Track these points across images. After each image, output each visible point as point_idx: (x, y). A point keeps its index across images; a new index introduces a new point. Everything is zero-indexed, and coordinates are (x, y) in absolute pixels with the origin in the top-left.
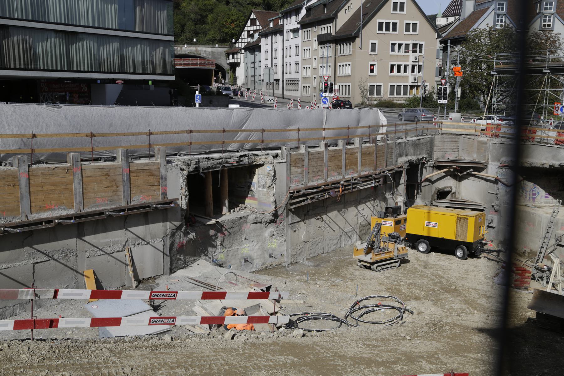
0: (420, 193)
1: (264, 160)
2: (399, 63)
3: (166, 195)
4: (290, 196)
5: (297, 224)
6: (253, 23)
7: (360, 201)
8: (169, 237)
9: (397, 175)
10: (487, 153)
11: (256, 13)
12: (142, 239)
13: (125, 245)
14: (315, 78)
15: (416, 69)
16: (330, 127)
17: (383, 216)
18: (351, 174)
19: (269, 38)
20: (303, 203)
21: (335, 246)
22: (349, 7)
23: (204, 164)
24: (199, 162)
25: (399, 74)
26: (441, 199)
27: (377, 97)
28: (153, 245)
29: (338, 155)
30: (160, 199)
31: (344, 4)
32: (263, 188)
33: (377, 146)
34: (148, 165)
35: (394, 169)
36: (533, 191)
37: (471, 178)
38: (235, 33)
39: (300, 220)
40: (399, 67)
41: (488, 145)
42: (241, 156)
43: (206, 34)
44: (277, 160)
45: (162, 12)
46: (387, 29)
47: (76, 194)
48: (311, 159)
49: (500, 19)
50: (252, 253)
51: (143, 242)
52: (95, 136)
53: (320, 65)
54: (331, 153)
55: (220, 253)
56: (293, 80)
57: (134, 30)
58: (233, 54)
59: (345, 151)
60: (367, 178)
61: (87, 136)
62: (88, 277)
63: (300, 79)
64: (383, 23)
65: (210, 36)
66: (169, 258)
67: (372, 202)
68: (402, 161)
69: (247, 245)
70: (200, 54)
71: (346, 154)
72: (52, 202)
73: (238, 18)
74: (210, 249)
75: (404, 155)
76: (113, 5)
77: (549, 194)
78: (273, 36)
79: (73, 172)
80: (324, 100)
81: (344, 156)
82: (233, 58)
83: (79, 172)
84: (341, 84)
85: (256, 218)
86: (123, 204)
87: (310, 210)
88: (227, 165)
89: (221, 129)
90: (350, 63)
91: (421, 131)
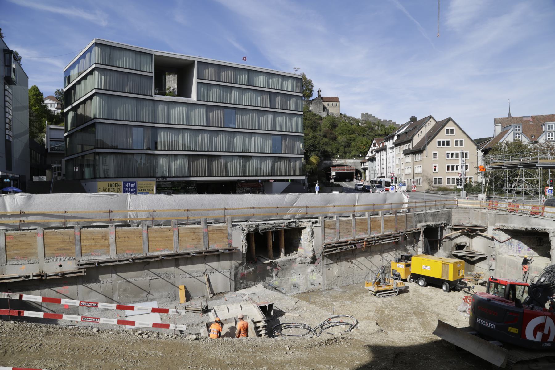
0: (442, 246)
1: (306, 225)
3: (232, 244)
4: (325, 247)
5: (331, 265)
6: (375, 146)
7: (384, 251)
8: (233, 269)
9: (416, 235)
11: (376, 140)
12: (215, 270)
13: (205, 272)
17: (398, 261)
19: (379, 153)
20: (334, 252)
21: (363, 280)
23: (262, 227)
24: (258, 226)
25: (453, 171)
26: (459, 249)
27: (439, 185)
28: (223, 273)
30: (228, 247)
33: (397, 216)
36: (518, 246)
37: (478, 236)
39: (333, 262)
40: (453, 167)
41: (487, 215)
44: (315, 225)
47: (174, 243)
48: (341, 224)
49: (518, 136)
50: (298, 282)
51: (216, 272)
52: (189, 211)
53: (405, 167)
55: (275, 280)
57: (280, 153)
58: (364, 163)
59: (369, 219)
60: (388, 236)
61: (185, 211)
62: (181, 290)
65: (353, 154)
66: (234, 282)
67: (394, 252)
68: (421, 226)
69: (295, 277)
71: (371, 221)
72: (161, 247)
73: (367, 143)
74: (268, 278)
77: (531, 248)
79: (173, 230)
80: (392, 188)
81: (369, 222)
82: (364, 165)
83: (177, 230)
84: (417, 178)
85: (301, 260)
86: (204, 249)
88: (279, 228)
89: (275, 206)
90: (421, 165)
91: (443, 206)
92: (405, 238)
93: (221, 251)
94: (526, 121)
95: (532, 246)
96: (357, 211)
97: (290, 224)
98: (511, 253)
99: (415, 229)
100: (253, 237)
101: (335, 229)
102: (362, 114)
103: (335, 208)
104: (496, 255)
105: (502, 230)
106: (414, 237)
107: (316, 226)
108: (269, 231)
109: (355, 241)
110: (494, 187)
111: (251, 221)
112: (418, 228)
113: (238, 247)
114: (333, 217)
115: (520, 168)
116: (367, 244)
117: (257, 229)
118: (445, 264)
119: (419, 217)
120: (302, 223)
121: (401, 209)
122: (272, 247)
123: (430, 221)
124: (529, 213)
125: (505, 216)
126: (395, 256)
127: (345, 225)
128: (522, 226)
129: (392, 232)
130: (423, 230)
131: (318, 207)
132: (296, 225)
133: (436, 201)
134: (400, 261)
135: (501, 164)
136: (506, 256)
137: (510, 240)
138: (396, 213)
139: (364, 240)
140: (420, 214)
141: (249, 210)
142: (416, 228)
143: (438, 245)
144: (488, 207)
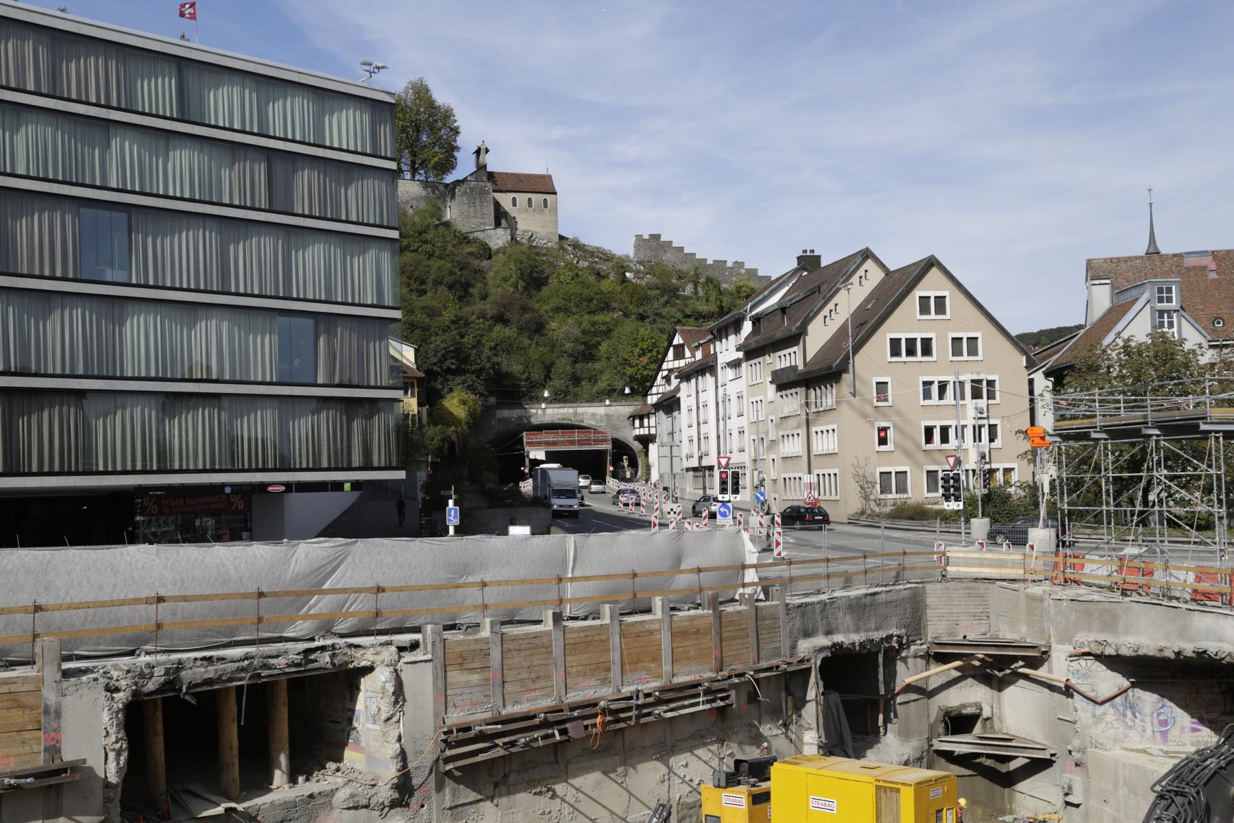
0: (895, 720)
1: (371, 658)
3: (59, 751)
4: (442, 741)
5: (471, 809)
6: (679, 354)
7: (674, 746)
9: (794, 681)
10: (1046, 624)
14: (773, 460)
16: (588, 574)
17: (723, 783)
18: (641, 682)
19: (693, 381)
22: (831, 311)
23: (195, 674)
24: (178, 670)
26: (954, 733)
27: (898, 496)
29: (596, 638)
30: (40, 762)
31: (819, 306)
32: (375, 722)
33: (719, 616)
34: (6, 683)
35: (778, 667)
36: (1159, 715)
37: (1021, 682)
38: (648, 375)
39: (480, 797)
41: (1046, 604)
42: (308, 652)
43: (596, 381)
44: (408, 657)
45: (377, 343)
46: (911, 352)
49: (1166, 320)
53: (781, 433)
54: (575, 635)
56: (739, 466)
57: (312, 381)
58: (641, 418)
59: (617, 629)
63: (747, 464)
64: (900, 339)
65: (602, 384)
67: (714, 747)
70: (582, 421)
71: (622, 635)
75: (820, 632)
76: (268, 336)
77: (1202, 721)
78: (700, 378)
80: (722, 510)
81: (615, 640)
82: (642, 426)
84: (821, 472)
85: (352, 796)
87: (510, 772)
88: (264, 673)
89: (253, 589)
90: (834, 427)
91: (894, 573)
92: (753, 697)
93: (6, 780)
94: (1194, 268)
95: (1205, 716)
96: (569, 601)
97: (312, 657)
98: (1135, 740)
99: (788, 660)
100: (159, 713)
101: (486, 668)
102: (639, 237)
103: (486, 589)
104: (1082, 750)
105: (1100, 658)
106: (787, 689)
107: (412, 659)
108: (227, 689)
109: (562, 711)
110: (1069, 504)
111: (148, 653)
112: (802, 655)
113: (84, 761)
114: (478, 625)
115: (1151, 436)
116: (610, 722)
117: (172, 682)
118: (885, 788)
119: (803, 615)
120: (360, 652)
121: (736, 587)
122: (235, 752)
123: (847, 631)
124: (1188, 597)
125: (1106, 606)
126: (715, 763)
127: (523, 653)
128: (1163, 645)
129: (702, 673)
130: (819, 663)
131: (421, 589)
132: (335, 661)
133: (790, 563)
134: (732, 780)
135: (1086, 423)
136: (1117, 752)
137: (1130, 692)
138: (715, 603)
139: (598, 709)
140: (807, 604)
141: (142, 607)
142: (792, 655)
143: (881, 717)
144: (1049, 574)
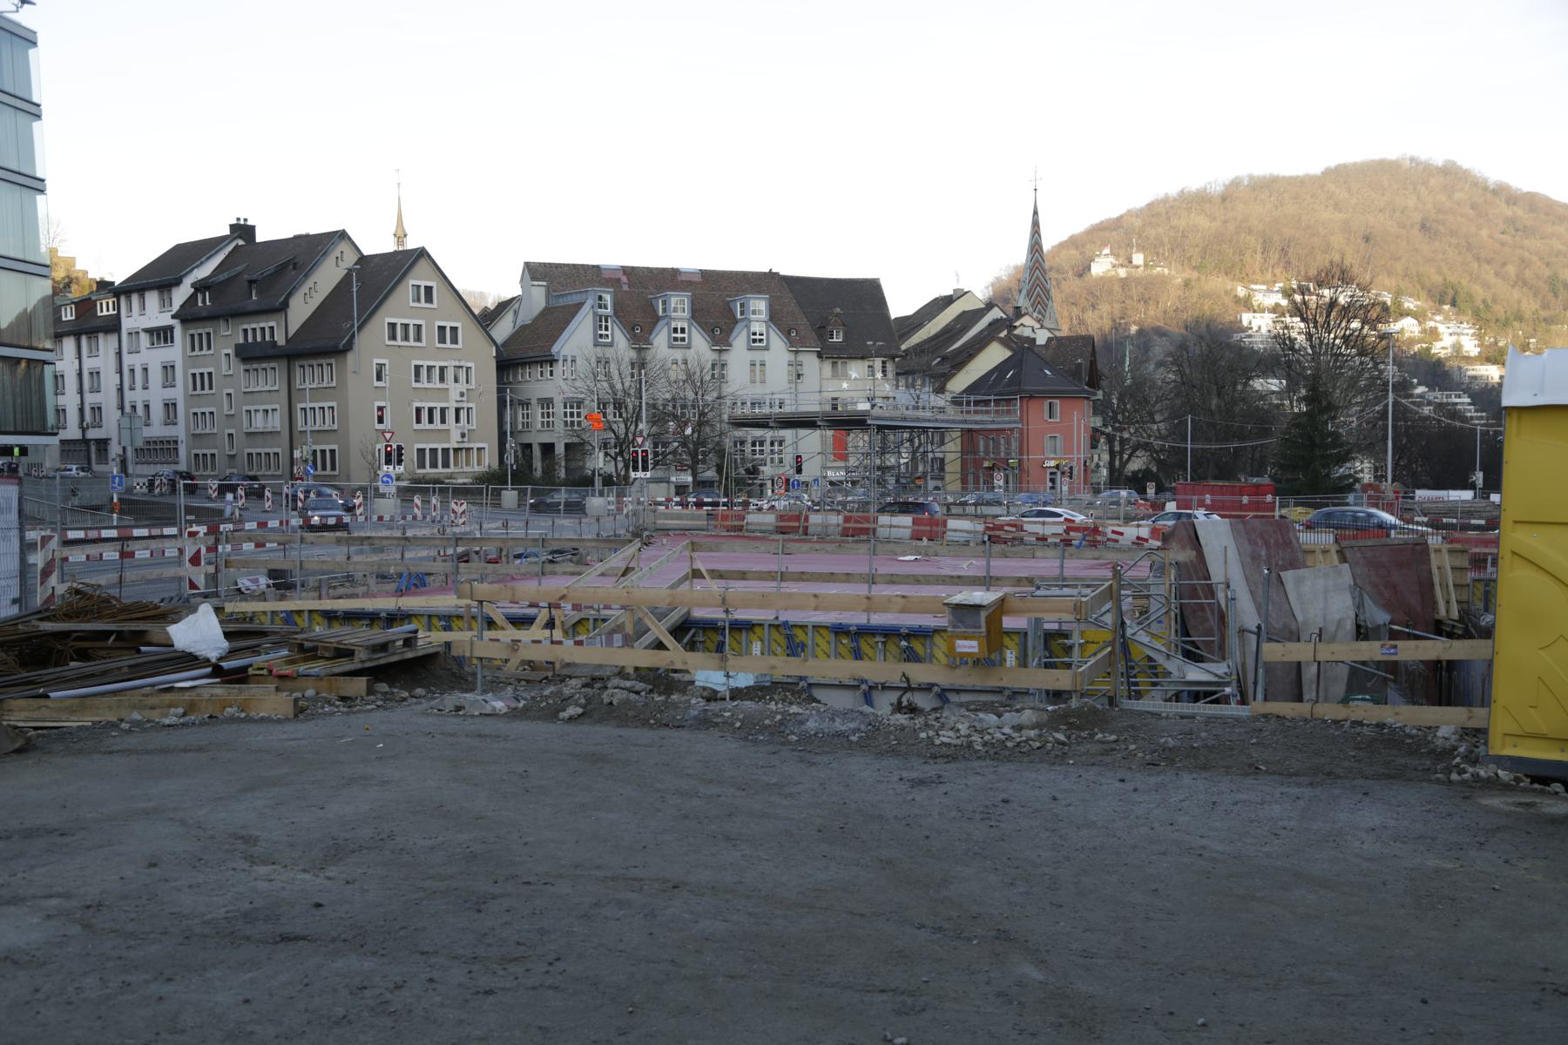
2: (432, 405)
15: (463, 414)
40: (431, 410)
53: (246, 408)
80: (385, 479)
